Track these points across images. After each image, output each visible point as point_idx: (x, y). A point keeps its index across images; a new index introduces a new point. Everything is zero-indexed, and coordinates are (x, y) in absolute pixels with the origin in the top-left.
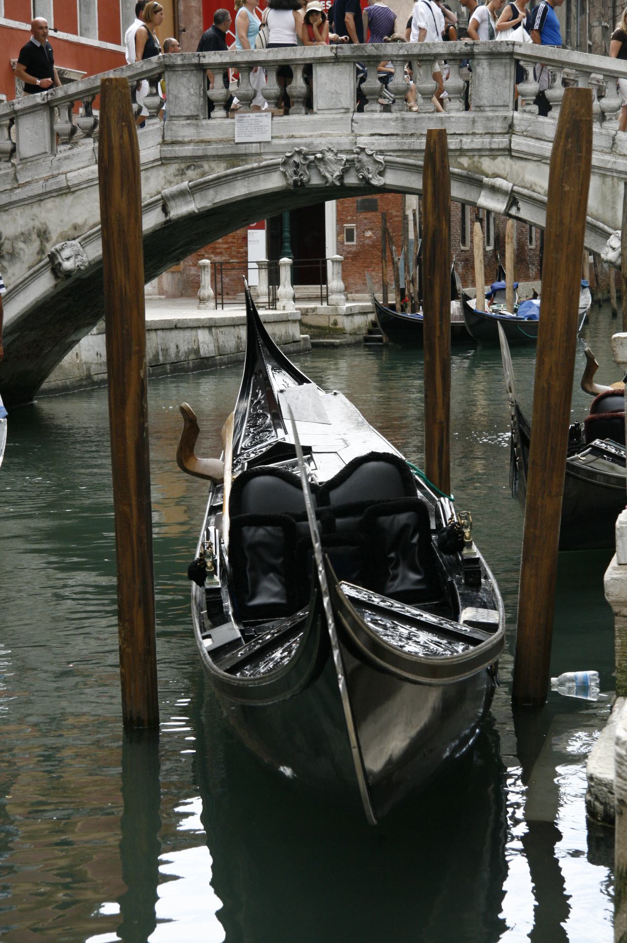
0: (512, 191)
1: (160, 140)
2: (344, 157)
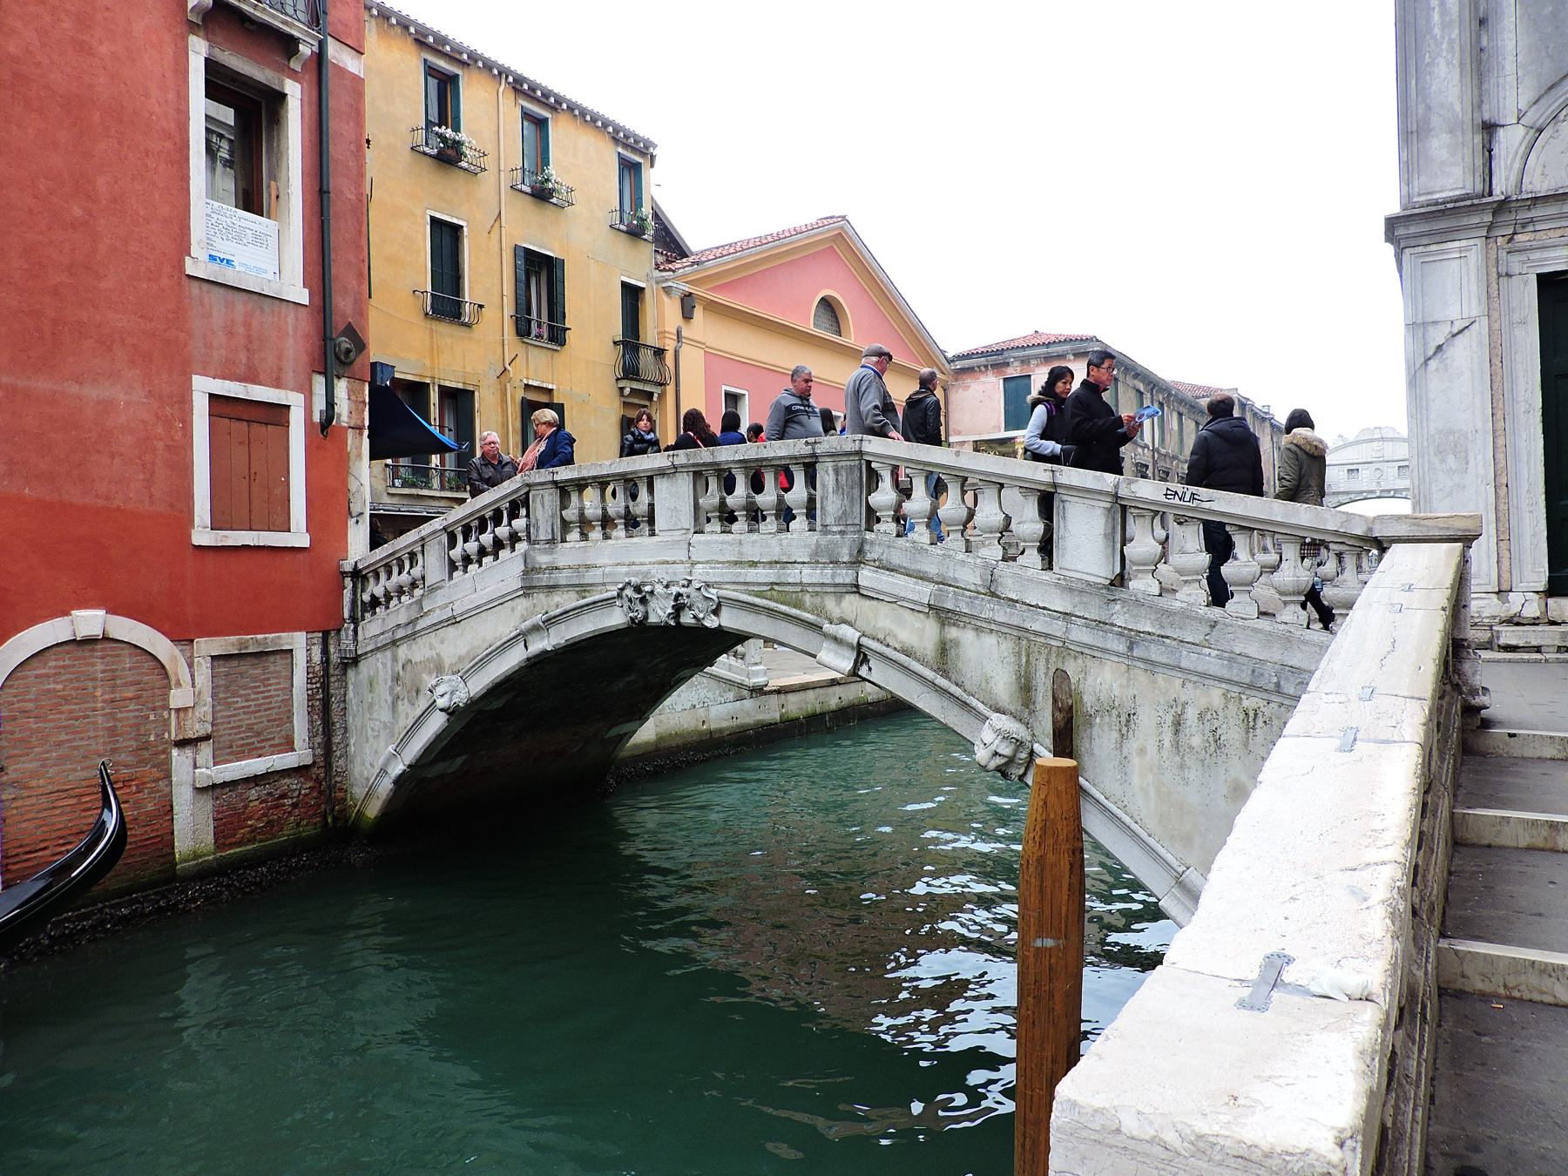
0: (859, 645)
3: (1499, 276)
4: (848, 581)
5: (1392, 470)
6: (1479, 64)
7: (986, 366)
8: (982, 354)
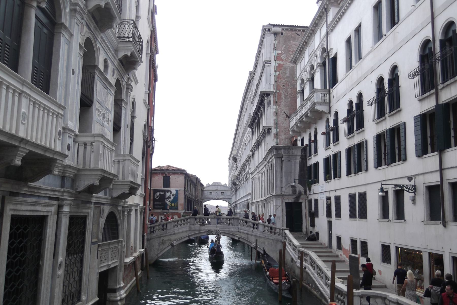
2: (216, 231)
5: (220, 193)
6: (281, 181)
7: (160, 173)
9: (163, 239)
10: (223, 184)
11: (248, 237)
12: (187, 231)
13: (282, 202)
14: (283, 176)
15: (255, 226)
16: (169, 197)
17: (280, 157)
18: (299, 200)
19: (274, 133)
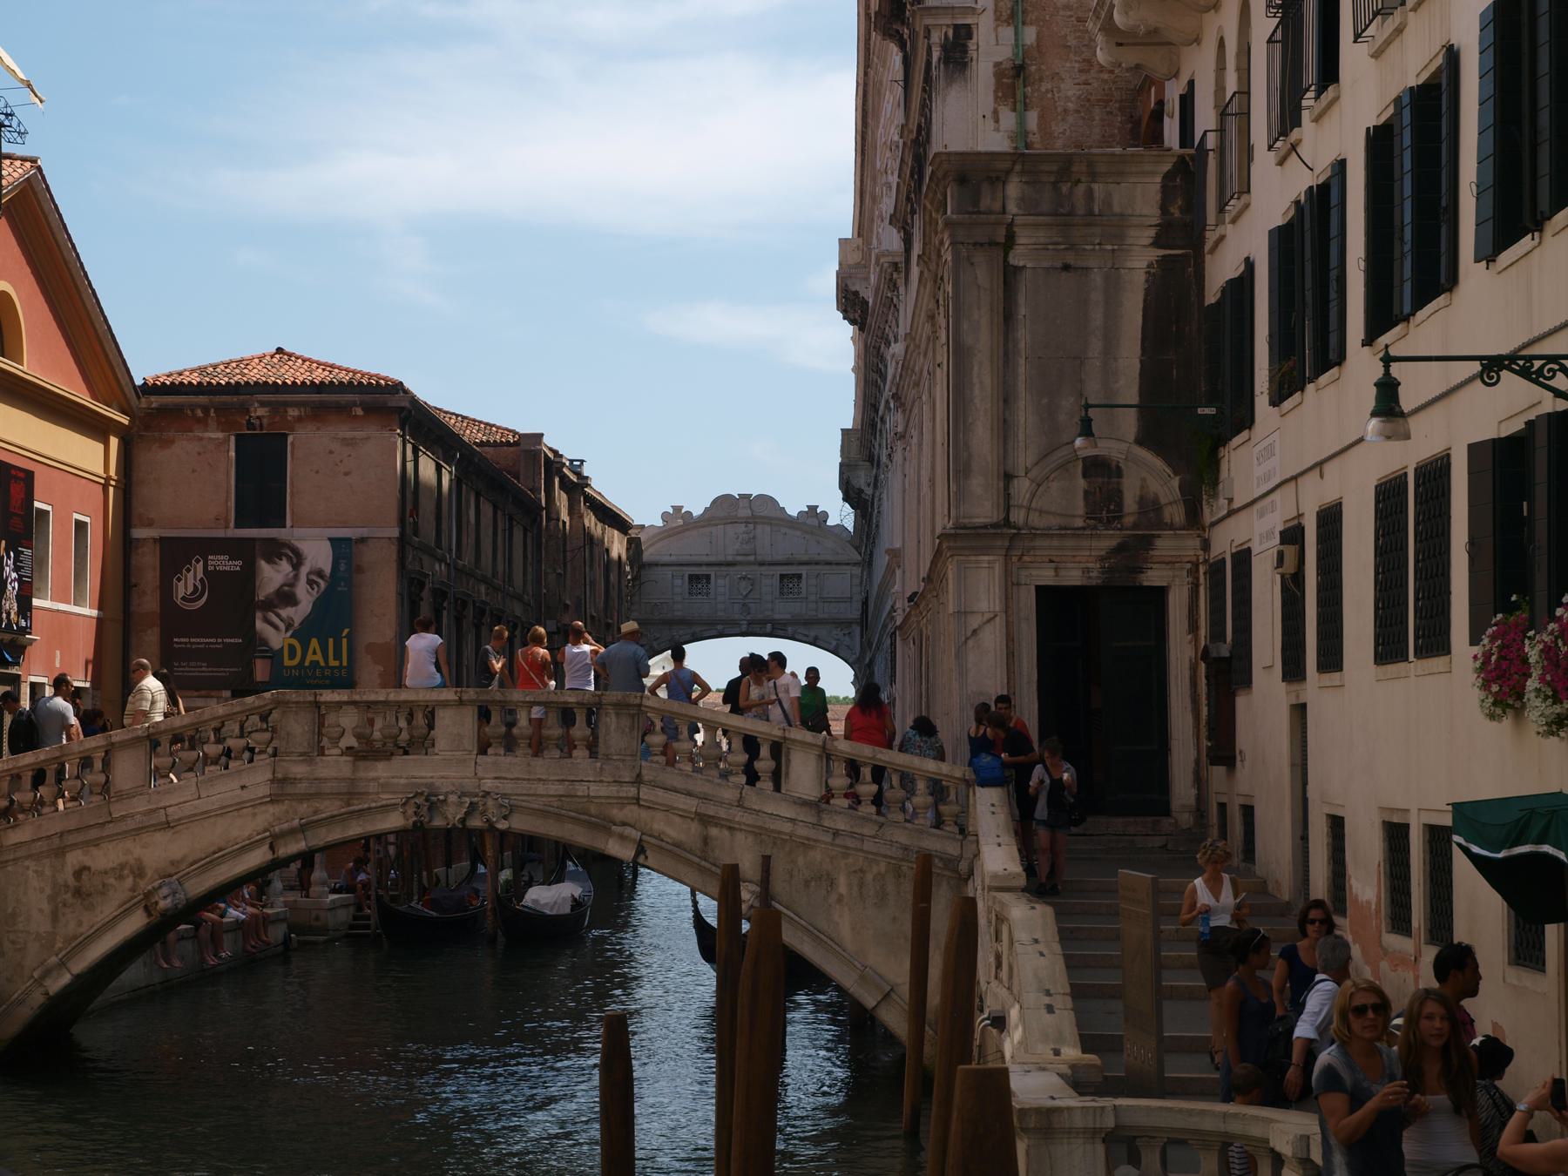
0: (641, 840)
1: (271, 777)
3: (1013, 584)
4: (630, 795)
5: (769, 582)
6: (1004, 429)
7: (206, 409)
8: (199, 389)
9: (87, 861)
10: (793, 508)
11: (706, 840)
12: (257, 803)
13: (1010, 585)
14: (1021, 387)
15: (764, 764)
16: (286, 597)
17: (993, 243)
18: (1141, 570)
19: (997, 65)
